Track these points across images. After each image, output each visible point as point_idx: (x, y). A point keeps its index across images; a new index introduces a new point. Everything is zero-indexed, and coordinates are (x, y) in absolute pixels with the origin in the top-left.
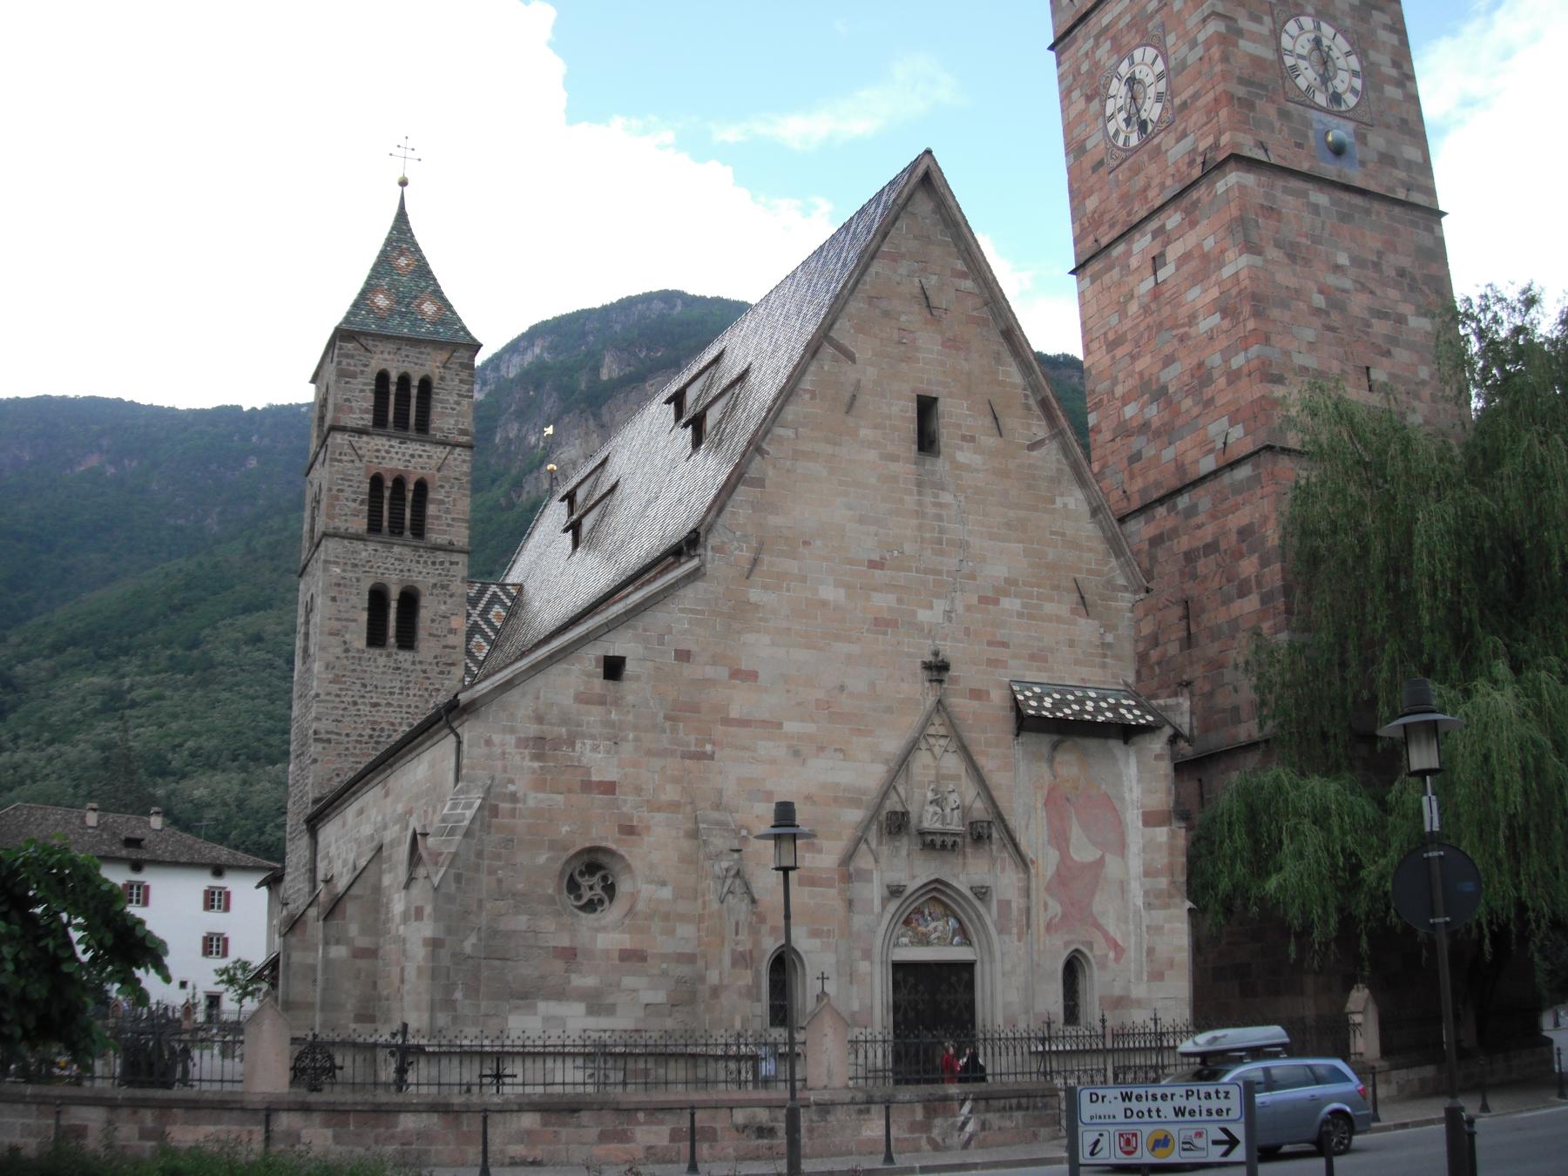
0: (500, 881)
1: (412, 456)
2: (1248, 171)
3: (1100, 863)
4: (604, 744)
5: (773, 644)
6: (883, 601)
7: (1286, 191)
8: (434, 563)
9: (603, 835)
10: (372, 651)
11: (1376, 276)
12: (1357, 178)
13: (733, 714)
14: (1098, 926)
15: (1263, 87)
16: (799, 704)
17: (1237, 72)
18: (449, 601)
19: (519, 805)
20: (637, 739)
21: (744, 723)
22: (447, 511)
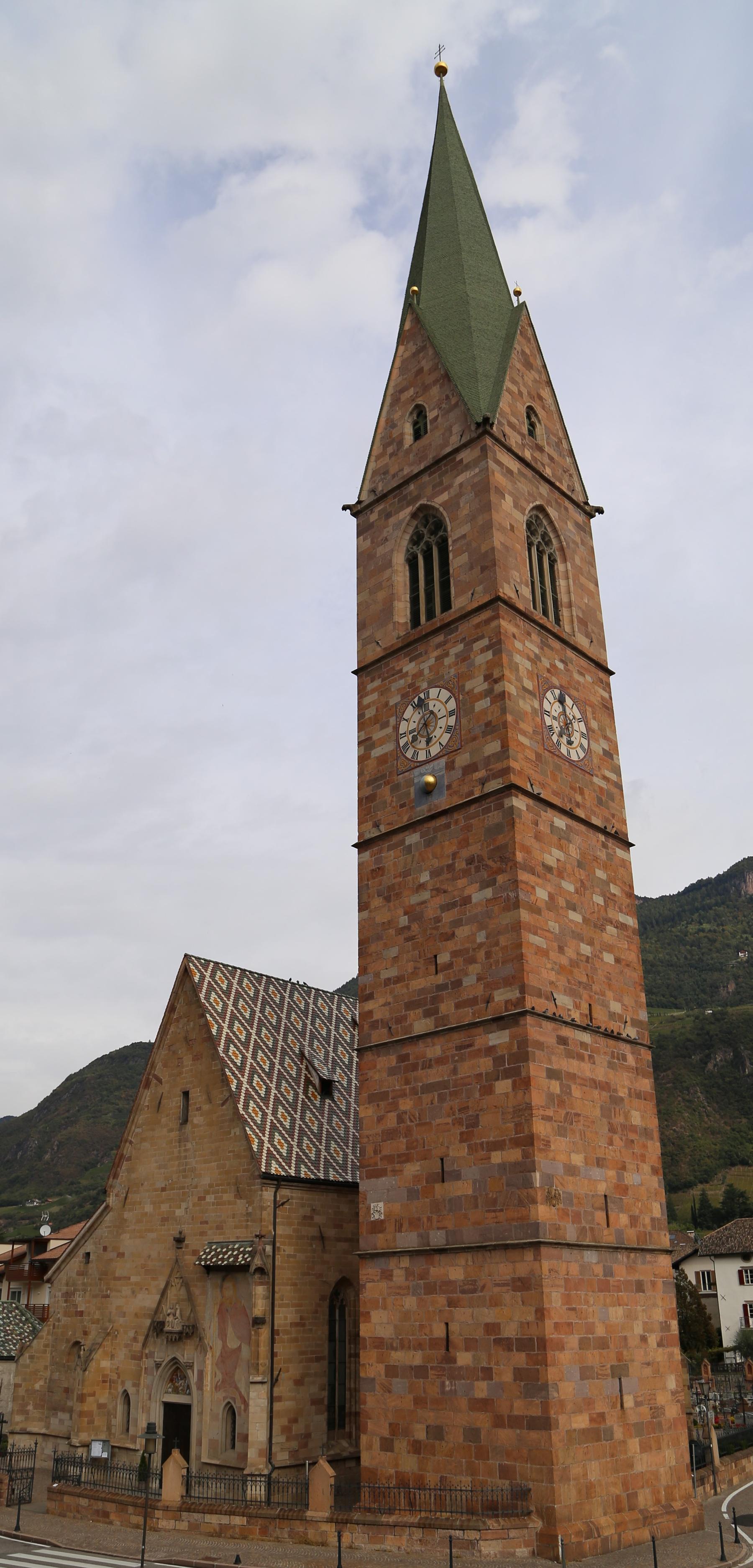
2: (366, 850)
3: (240, 1348)
4: (82, 1293)
5: (130, 1238)
6: (165, 1207)
7: (389, 849)
11: (449, 876)
12: (442, 801)
13: (117, 1275)
14: (237, 1388)
15: (383, 776)
17: (368, 778)
21: (119, 1279)
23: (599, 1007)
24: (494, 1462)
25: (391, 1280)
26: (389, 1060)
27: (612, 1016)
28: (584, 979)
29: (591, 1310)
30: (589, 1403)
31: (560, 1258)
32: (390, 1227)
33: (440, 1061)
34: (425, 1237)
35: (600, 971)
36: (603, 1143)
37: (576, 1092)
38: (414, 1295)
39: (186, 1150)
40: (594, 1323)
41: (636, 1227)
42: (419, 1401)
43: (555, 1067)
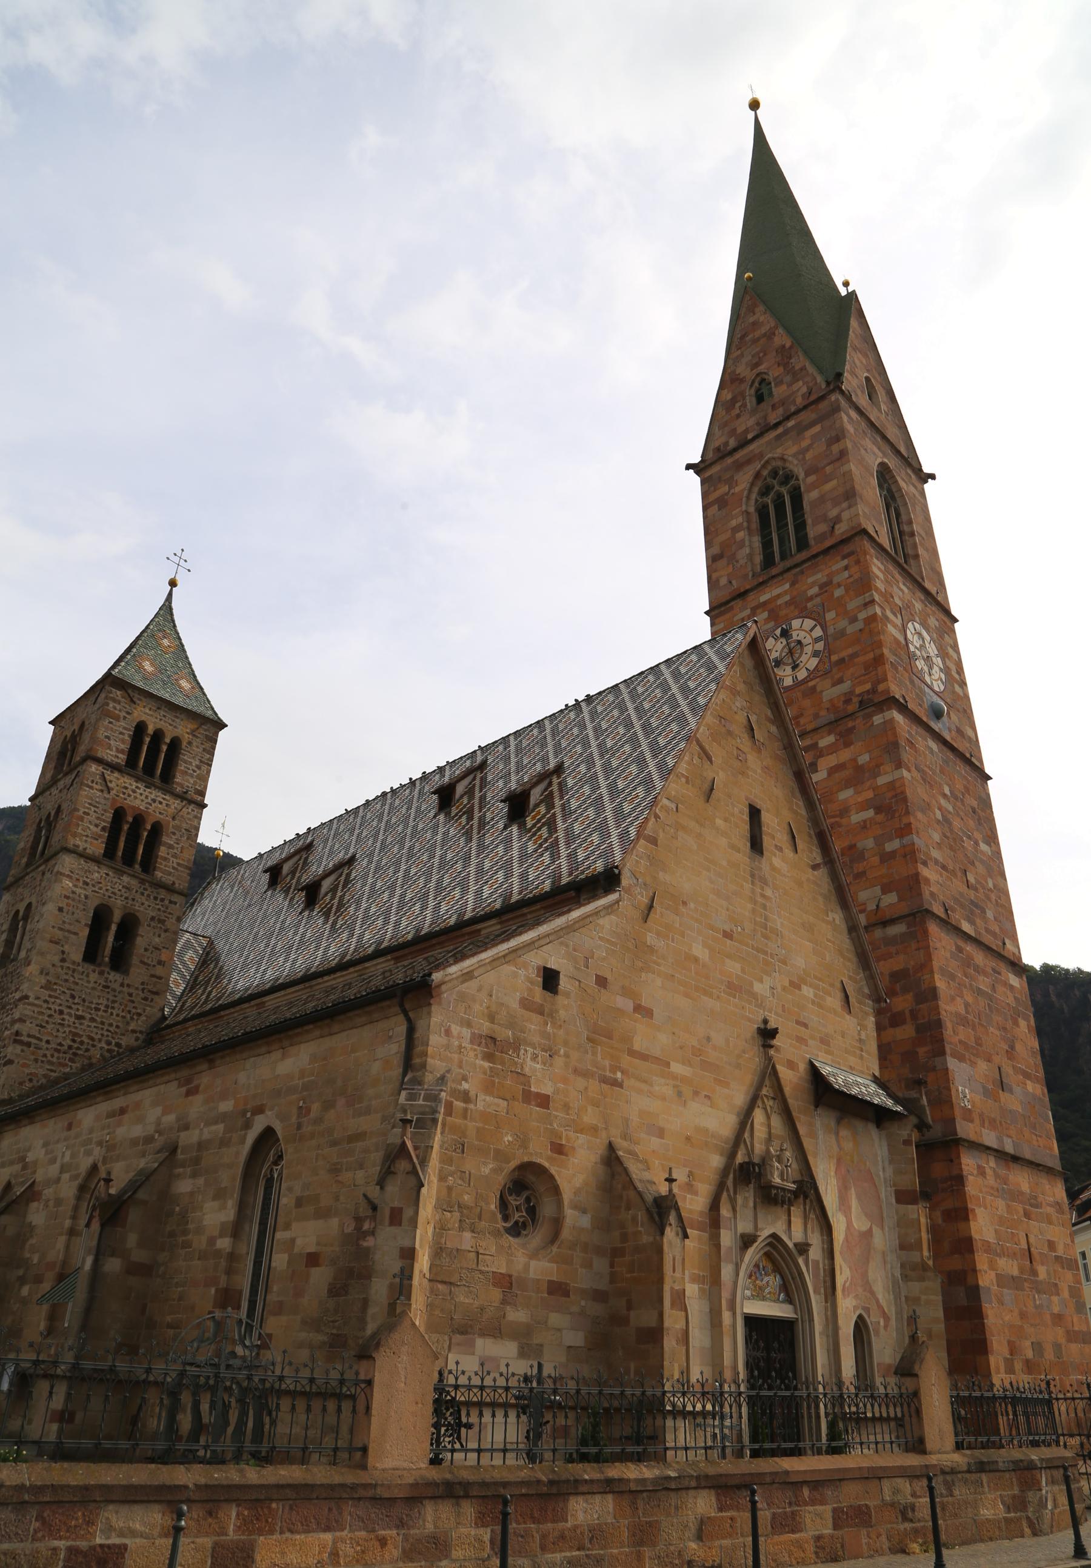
0: (450, 1189)
1: (154, 801)
6: (734, 967)
8: (156, 898)
9: (539, 1153)
10: (86, 965)
16: (681, 1048)
18: (163, 935)
19: (471, 1106)
20: (567, 1056)
21: (644, 1057)
22: (175, 856)
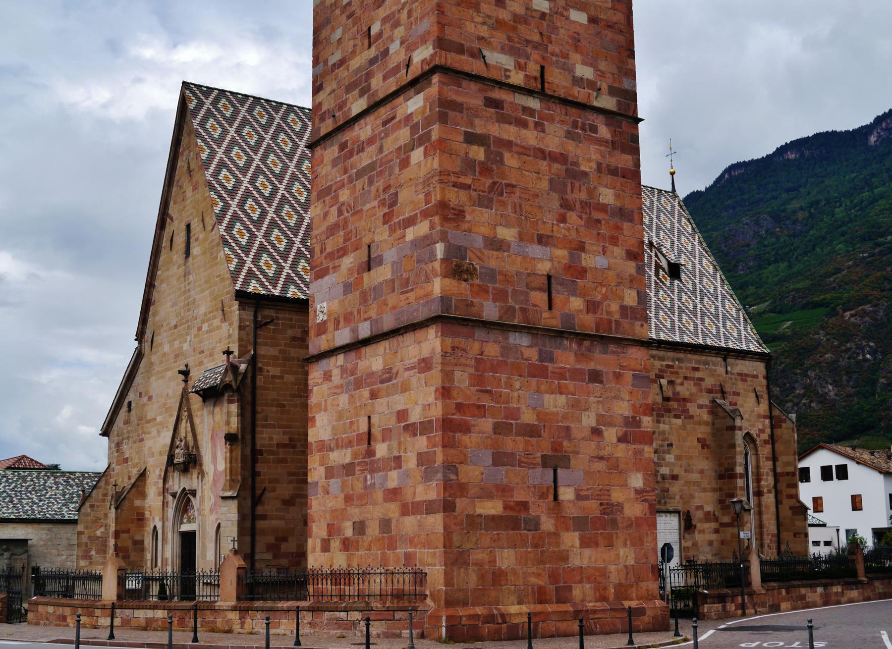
23: (557, 71)
24: (400, 551)
25: (331, 380)
26: (331, 152)
27: (578, 81)
28: (536, 38)
29: (515, 394)
30: (503, 490)
31: (472, 336)
32: (331, 326)
33: (370, 141)
34: (354, 331)
35: (562, 31)
36: (550, 219)
37: (511, 160)
38: (346, 392)
39: (189, 284)
40: (518, 409)
41: (595, 313)
42: (348, 499)
43: (478, 131)
